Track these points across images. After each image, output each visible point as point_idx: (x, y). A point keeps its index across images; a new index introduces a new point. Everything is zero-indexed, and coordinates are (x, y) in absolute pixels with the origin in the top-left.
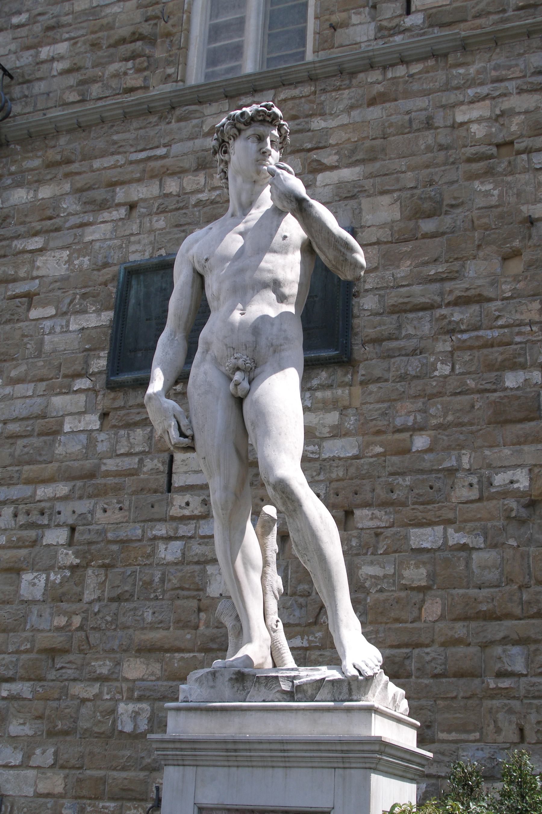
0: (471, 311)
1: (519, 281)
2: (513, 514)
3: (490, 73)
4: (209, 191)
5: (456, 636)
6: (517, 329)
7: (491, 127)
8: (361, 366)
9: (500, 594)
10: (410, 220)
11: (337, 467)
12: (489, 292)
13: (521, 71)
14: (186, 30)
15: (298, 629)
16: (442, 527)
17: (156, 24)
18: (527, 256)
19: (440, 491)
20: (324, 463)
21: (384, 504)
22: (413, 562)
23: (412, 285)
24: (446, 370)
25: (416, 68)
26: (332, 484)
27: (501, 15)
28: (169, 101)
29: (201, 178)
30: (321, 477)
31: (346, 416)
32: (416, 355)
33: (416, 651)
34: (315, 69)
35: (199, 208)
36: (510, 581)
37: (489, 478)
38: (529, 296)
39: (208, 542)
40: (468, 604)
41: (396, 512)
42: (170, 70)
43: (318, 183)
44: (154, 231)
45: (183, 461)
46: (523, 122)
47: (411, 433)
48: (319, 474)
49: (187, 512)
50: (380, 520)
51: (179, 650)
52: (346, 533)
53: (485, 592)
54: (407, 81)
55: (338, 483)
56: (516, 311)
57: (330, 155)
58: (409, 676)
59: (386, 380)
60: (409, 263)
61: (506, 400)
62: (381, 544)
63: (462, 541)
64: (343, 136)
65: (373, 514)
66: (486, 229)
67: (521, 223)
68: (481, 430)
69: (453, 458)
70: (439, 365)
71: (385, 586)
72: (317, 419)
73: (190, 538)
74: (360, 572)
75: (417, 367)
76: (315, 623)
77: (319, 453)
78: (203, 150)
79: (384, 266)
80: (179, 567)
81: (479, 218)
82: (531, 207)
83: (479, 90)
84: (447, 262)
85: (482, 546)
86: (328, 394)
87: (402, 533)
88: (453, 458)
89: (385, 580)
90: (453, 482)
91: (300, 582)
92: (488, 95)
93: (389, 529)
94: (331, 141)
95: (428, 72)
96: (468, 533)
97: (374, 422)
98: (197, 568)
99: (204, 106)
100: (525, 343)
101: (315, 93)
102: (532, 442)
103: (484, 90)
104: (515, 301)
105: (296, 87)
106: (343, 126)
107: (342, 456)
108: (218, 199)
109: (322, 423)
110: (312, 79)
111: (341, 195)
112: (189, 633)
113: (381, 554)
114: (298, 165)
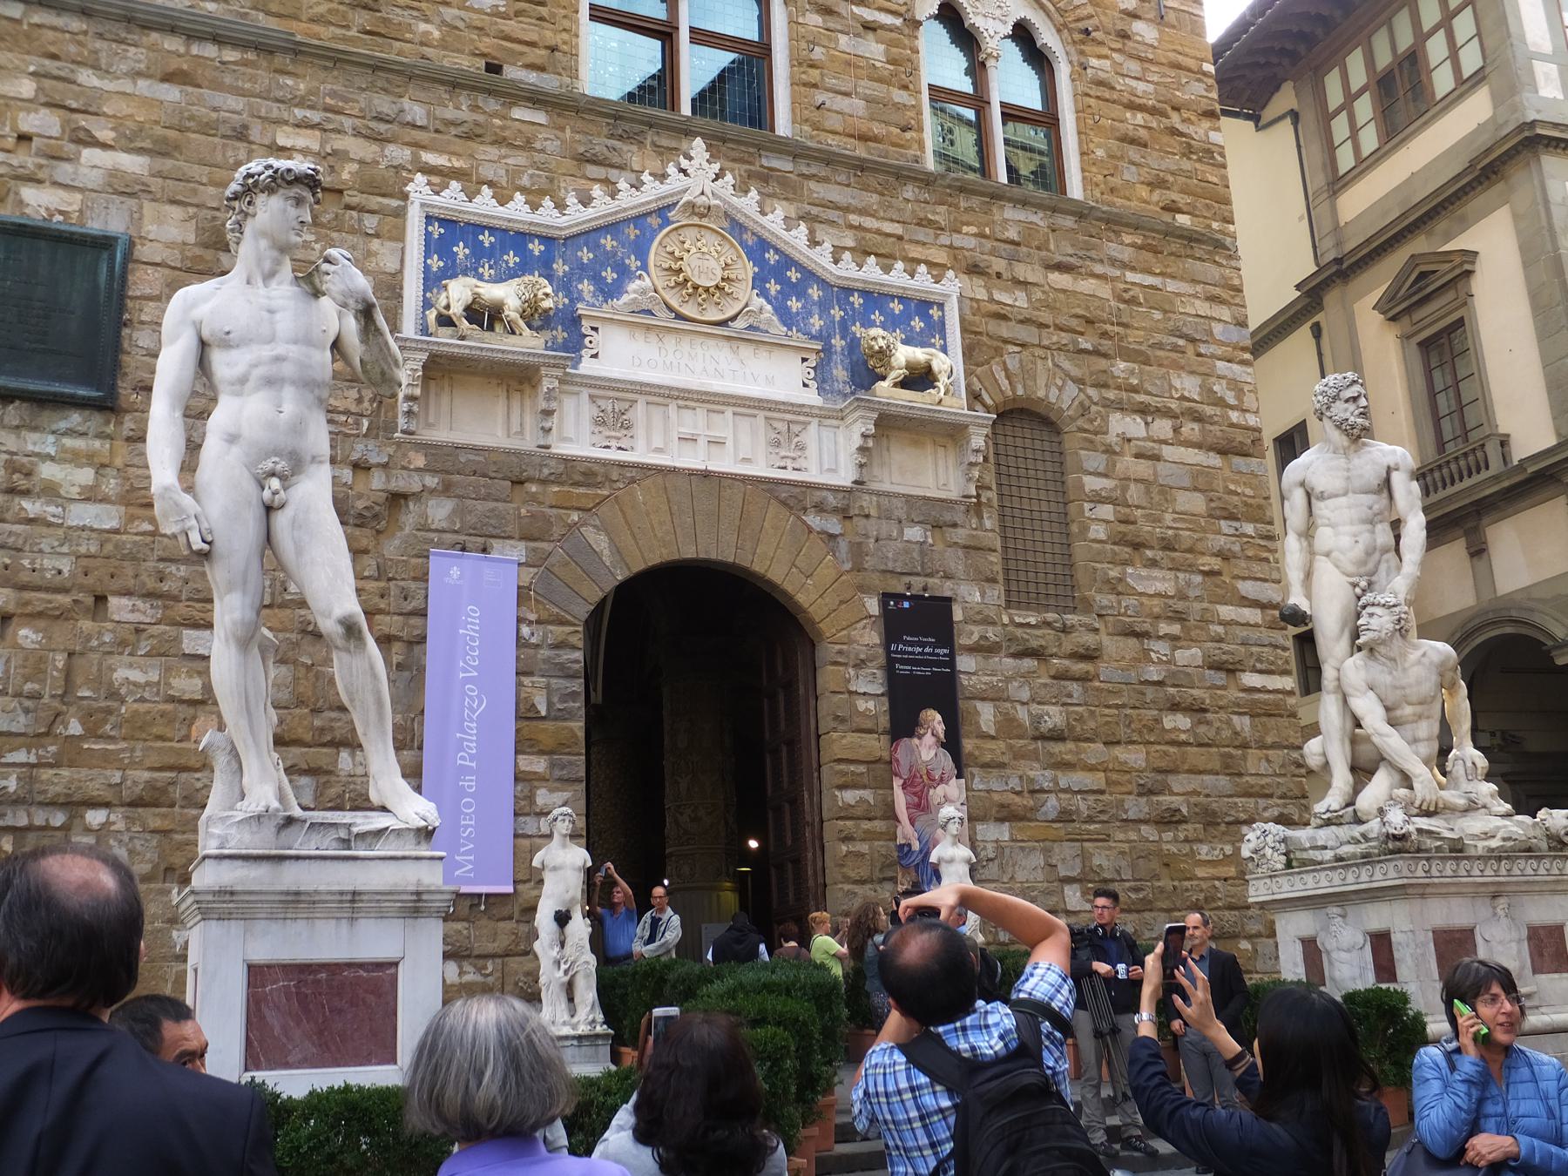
2: (310, 628)
8: (128, 417)
13: (361, 110)
15: (21, 739)
21: (150, 595)
25: (231, 55)
30: (65, 549)
33: (184, 776)
36: (300, 703)
37: (283, 583)
43: (83, 160)
48: (61, 545)
58: (172, 805)
62: (143, 644)
64: (123, 108)
71: (146, 695)
74: (115, 675)
76: (47, 734)
83: (309, 113)
91: (27, 679)
101: (85, 33)
103: (315, 116)
105: (59, 15)
106: (124, 94)
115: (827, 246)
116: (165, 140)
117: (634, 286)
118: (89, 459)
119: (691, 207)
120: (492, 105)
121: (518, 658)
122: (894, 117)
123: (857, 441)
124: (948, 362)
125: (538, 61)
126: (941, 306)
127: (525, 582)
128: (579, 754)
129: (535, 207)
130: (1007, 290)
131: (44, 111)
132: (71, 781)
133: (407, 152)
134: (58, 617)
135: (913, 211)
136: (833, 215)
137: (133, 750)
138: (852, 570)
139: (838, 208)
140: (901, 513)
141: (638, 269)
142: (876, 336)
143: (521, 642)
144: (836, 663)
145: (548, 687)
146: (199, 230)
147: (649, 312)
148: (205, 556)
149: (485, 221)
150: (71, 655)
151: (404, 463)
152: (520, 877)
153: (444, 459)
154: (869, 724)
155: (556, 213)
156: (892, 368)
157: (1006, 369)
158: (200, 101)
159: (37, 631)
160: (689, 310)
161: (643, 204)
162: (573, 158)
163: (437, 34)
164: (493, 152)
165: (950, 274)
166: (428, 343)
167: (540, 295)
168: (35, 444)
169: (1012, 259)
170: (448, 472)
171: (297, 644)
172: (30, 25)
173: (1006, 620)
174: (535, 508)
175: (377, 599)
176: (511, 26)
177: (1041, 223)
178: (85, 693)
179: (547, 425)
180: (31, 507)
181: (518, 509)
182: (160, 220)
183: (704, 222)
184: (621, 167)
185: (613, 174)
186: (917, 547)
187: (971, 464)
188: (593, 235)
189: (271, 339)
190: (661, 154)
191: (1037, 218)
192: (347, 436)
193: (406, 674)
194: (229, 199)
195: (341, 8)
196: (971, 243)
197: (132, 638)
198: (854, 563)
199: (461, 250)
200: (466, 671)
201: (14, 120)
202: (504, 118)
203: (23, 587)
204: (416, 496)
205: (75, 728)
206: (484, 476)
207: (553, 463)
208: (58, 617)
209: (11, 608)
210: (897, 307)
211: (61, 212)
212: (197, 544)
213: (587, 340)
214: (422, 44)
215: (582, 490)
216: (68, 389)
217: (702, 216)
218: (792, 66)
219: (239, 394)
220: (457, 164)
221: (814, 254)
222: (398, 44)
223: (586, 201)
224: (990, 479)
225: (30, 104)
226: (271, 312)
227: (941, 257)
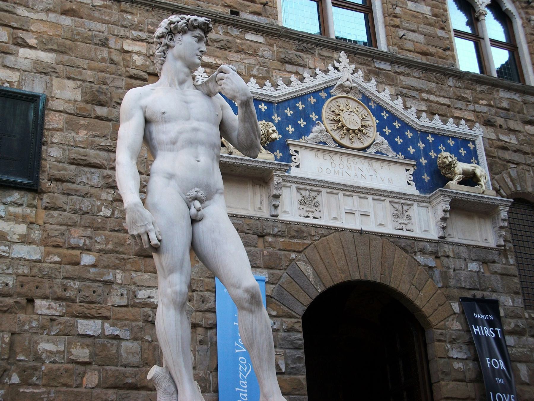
3: (147, 26)
7: (146, 61)
8: (45, 196)
9: (140, 373)
10: (88, 103)
11: (23, 266)
16: (101, 321)
19: (101, 296)
20: (13, 261)
21: (59, 299)
22: (79, 344)
23: (86, 148)
24: (108, 213)
26: (18, 277)
30: (10, 271)
31: (32, 229)
32: (87, 197)
37: (134, 292)
40: (118, 378)
41: (68, 306)
43: (20, 55)
47: (81, 251)
48: (8, 269)
50: (56, 310)
52: (28, 316)
54: (91, 9)
55: (24, 277)
57: (32, 38)
59: (65, 211)
60: (85, 132)
62: (54, 328)
63: (115, 334)
65: (49, 305)
68: (130, 258)
69: (111, 274)
70: (103, 208)
71: (57, 359)
74: (39, 347)
75: (89, 206)
77: (9, 253)
79: (67, 129)
83: (140, 34)
84: (111, 139)
85: (128, 338)
86: (18, 210)
87: (71, 322)
88: (111, 274)
89: (57, 355)
90: (110, 291)
92: (146, 39)
93: (62, 318)
94: (32, 28)
95: (106, 8)
96: (120, 327)
97: (54, 238)
107: (27, 258)
109: (13, 231)
111: (38, 69)
113: (54, 335)
114: (5, 36)
115: (413, 109)
116: (64, 45)
117: (316, 129)
118: (24, 219)
119: (341, 86)
120: (235, 32)
122: (439, 43)
123: (441, 214)
124: (482, 170)
125: (258, 10)
126: (474, 142)
128: (304, 395)
129: (262, 86)
130: (505, 134)
134: (5, 312)
135: (454, 92)
136: (414, 93)
137: (49, 393)
138: (442, 287)
139: (416, 90)
140: (465, 255)
141: (317, 120)
142: (446, 156)
144: (439, 341)
145: (284, 354)
146: (84, 93)
147: (324, 143)
148: (157, 249)
150: (13, 334)
154: (461, 377)
155: (272, 89)
156: (455, 174)
157: (510, 176)
158: (82, 25)
160: (345, 142)
161: (317, 85)
162: (279, 61)
165: (477, 125)
167: (270, 130)
169: (506, 118)
171: (141, 329)
173: (527, 316)
174: (271, 250)
177: (519, 99)
178: (21, 357)
179: (276, 203)
181: (262, 251)
182: (62, 87)
183: (349, 95)
184: (304, 66)
185: (300, 70)
186: (476, 274)
187: (501, 228)
188: (292, 102)
189: (188, 119)
190: (324, 60)
191: (516, 97)
193: (205, 347)
194: (159, 37)
196: (485, 109)
197: (48, 324)
198: (444, 283)
202: (241, 39)
205: (15, 379)
210: (451, 142)
211: (8, 82)
212: (154, 241)
213: (293, 157)
215: (296, 241)
216: (13, 179)
217: (348, 92)
218: (385, 17)
219: (171, 150)
221: (407, 113)
223: (288, 83)
224: (509, 236)
226: (186, 102)
227: (471, 116)
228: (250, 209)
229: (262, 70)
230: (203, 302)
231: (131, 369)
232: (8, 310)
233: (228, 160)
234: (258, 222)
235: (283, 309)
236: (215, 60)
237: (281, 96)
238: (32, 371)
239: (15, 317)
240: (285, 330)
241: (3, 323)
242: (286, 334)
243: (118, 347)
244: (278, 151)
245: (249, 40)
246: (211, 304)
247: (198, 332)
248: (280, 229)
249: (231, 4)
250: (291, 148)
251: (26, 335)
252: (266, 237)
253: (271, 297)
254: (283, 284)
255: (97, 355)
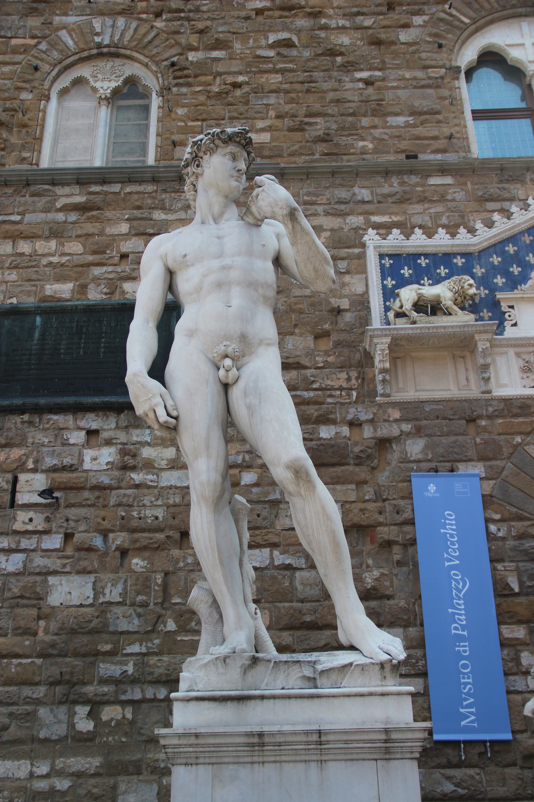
0: (291, 375)
1: (330, 356)
4: (60, 256)
5: (284, 643)
6: (328, 393)
9: (321, 608)
11: (174, 494)
12: (305, 361)
13: (328, 199)
14: (41, 125)
16: (269, 549)
17: (13, 116)
18: (334, 337)
27: (311, 157)
28: (25, 178)
29: (53, 244)
30: (160, 502)
34: (159, 172)
35: (51, 269)
38: (338, 368)
39: (50, 555)
42: (25, 155)
44: (6, 282)
45: (27, 481)
46: (329, 237)
48: (157, 500)
49: (30, 528)
51: (17, 656)
52: (182, 551)
53: (308, 605)
55: (175, 508)
56: (328, 378)
61: (321, 448)
63: (287, 562)
66: (301, 313)
67: (329, 311)
72: (156, 453)
73: (33, 551)
76: (153, 631)
77: (158, 482)
78: (55, 222)
80: (21, 578)
81: (295, 304)
82: (337, 300)
85: (304, 566)
88: (277, 492)
90: (277, 513)
91: (138, 593)
96: (292, 555)
98: (39, 578)
99: (57, 187)
100: (335, 404)
101: (156, 191)
102: (343, 483)
104: (326, 370)
105: (140, 185)
106: (181, 220)
107: (178, 485)
108: (67, 264)
109: (161, 457)
110: (154, 180)
112: (27, 640)
120: (414, 179)
121: (490, 549)
125: (442, 147)
127: (487, 491)
129: (453, 235)
131: (134, 239)
132: (169, 665)
133: (361, 218)
134: (157, 549)
143: (490, 537)
149: (420, 250)
150: (166, 574)
151: (386, 417)
152: (517, 727)
153: (413, 411)
155: (469, 235)
159: (143, 560)
162: (475, 201)
163: (371, 146)
164: (419, 208)
166: (389, 330)
167: (466, 286)
168: (138, 436)
170: (417, 419)
172: (124, 193)
174: (486, 436)
175: (376, 516)
176: (420, 131)
179: (486, 375)
180: (137, 477)
181: (474, 439)
184: (512, 200)
185: (506, 205)
192: (342, 404)
193: (405, 569)
195: (308, 144)
199: (406, 272)
200: (451, 560)
201: (118, 247)
202: (423, 185)
203: (133, 531)
204: (397, 439)
205: (171, 626)
206: (445, 419)
207: (495, 403)
208: (157, 549)
209: (126, 545)
213: (506, 315)
214: (362, 153)
215: (521, 419)
220: (395, 219)
222: (345, 157)
223: (490, 224)
225: (127, 236)
228: (452, 388)
229: (453, 216)
230: (398, 513)
231: (309, 604)
232: (159, 546)
233: (410, 332)
234: (465, 403)
235: (509, 510)
236: (390, 218)
237: (481, 243)
238: (190, 615)
239: (168, 554)
240: (515, 536)
241: (155, 562)
242: (516, 543)
243: (292, 579)
244: (485, 310)
245: (432, 185)
246: (408, 514)
247: (394, 551)
248: (496, 408)
249: (405, 148)
250: (502, 304)
251: (181, 574)
252: (478, 421)
253: (491, 496)
254: (507, 477)
255: (266, 590)
